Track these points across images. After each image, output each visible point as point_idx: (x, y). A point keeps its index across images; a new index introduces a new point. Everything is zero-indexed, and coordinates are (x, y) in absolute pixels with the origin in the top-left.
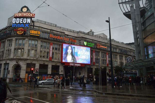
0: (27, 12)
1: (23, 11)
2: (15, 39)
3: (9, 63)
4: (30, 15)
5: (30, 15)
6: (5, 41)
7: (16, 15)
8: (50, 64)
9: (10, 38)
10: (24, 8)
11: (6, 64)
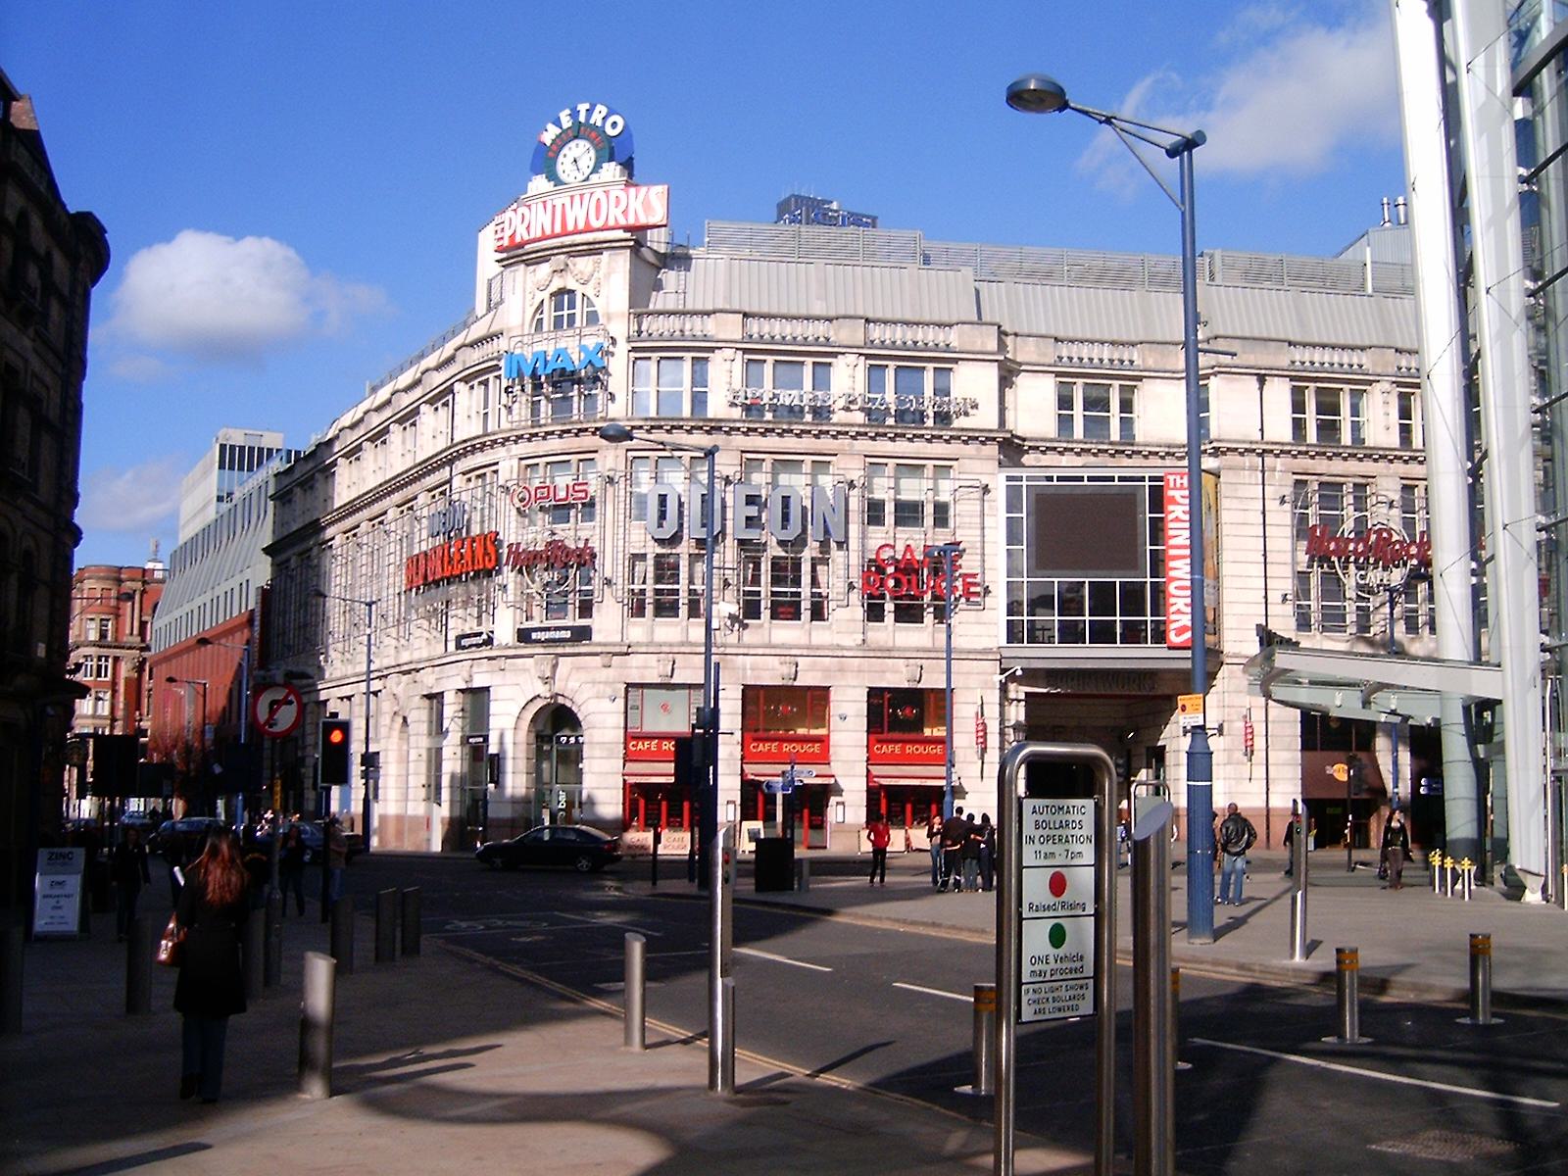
0: (594, 178)
1: (563, 177)
2: (515, 462)
3: (487, 689)
4: (625, 212)
5: (625, 212)
6: (449, 481)
7: (508, 233)
8: (851, 679)
9: (479, 459)
10: (565, 150)
11: (477, 698)
